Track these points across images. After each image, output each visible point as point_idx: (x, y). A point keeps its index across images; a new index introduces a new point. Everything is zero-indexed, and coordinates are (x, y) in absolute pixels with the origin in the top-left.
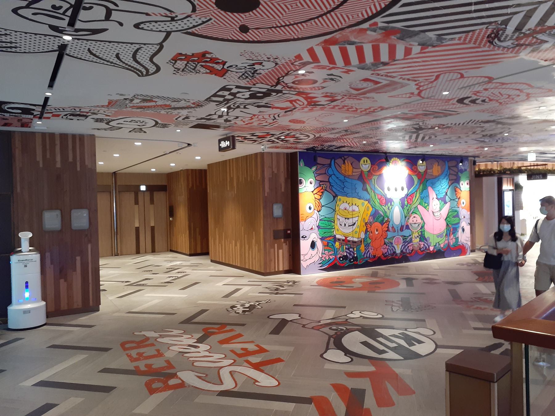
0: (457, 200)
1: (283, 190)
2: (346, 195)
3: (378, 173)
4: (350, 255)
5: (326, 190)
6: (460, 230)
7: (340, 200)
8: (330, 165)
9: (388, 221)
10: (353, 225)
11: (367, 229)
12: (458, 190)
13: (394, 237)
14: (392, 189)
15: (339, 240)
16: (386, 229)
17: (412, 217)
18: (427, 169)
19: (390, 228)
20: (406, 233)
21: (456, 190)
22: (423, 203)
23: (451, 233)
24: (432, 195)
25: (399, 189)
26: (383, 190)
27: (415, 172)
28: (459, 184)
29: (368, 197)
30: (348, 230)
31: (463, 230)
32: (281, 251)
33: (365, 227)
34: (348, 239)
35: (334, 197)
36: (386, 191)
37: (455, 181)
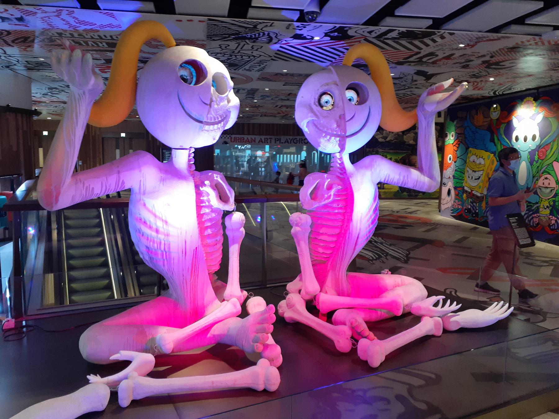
2: (476, 147)
3: (506, 121)
4: (473, 209)
5: (461, 142)
10: (478, 179)
14: (521, 139)
15: (466, 191)
26: (510, 139)
30: (474, 184)
34: (473, 192)
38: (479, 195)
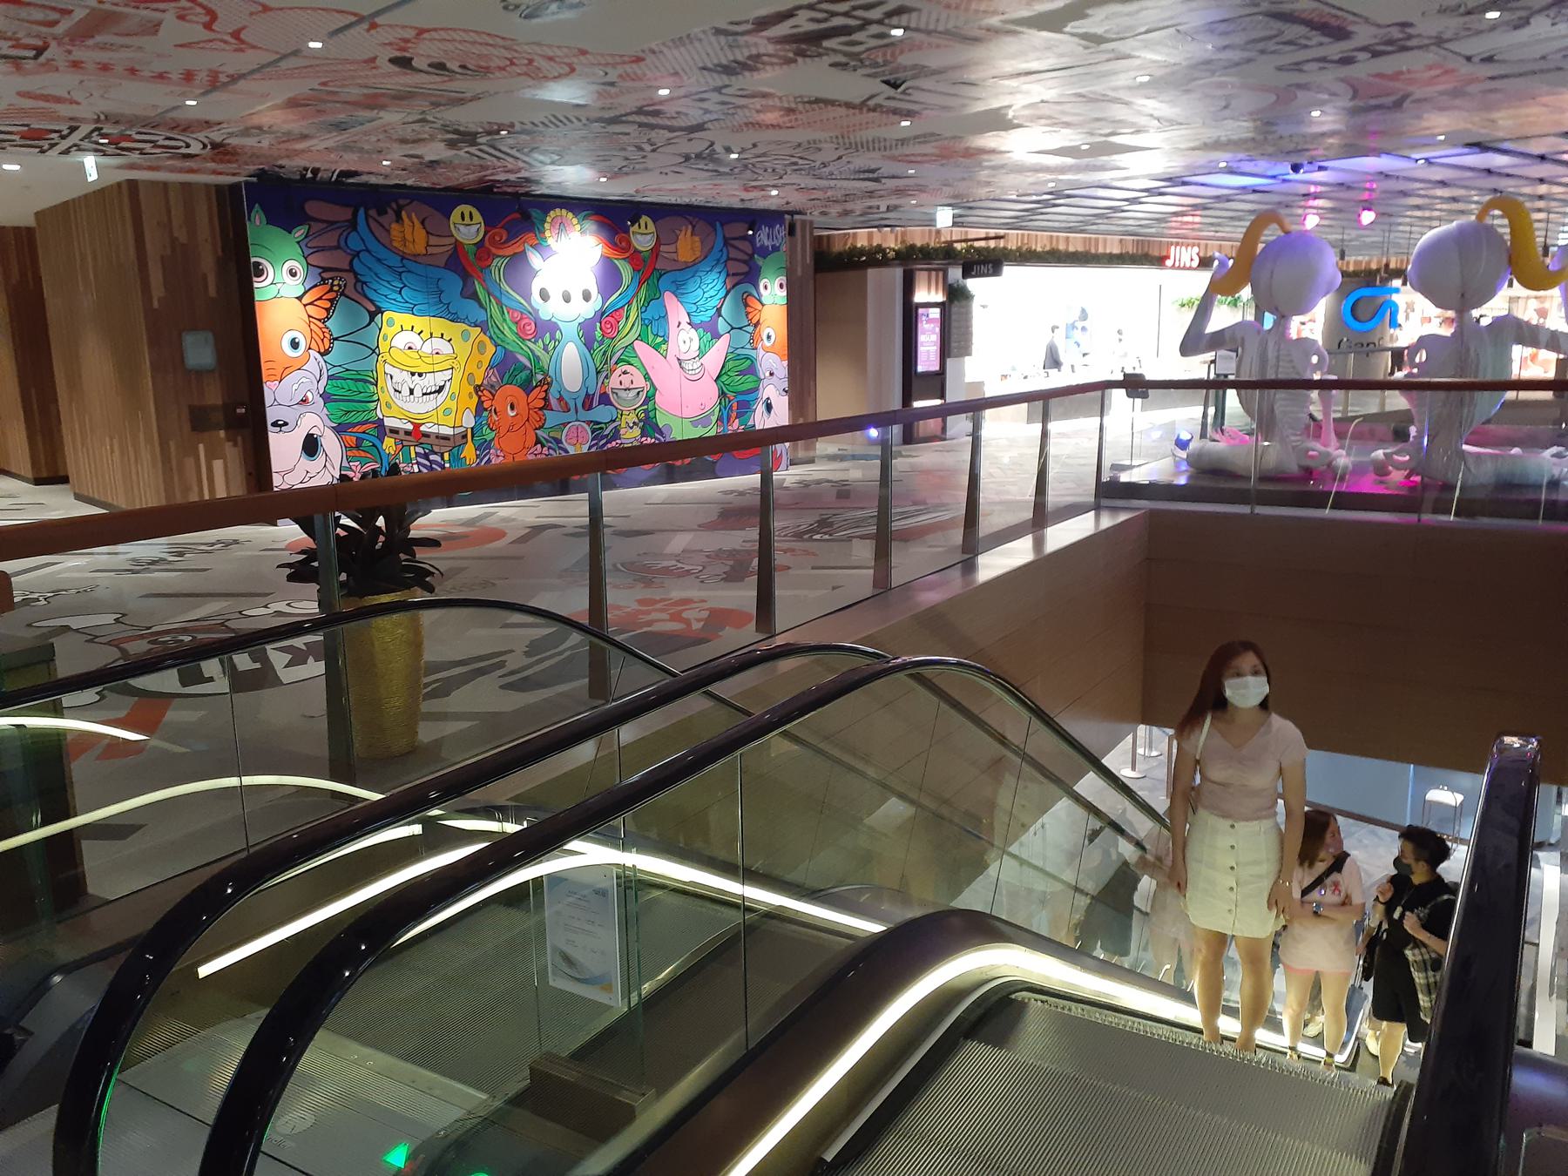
0: (750, 329)
1: (212, 292)
5: (343, 294)
6: (760, 408)
7: (391, 323)
8: (353, 225)
9: (546, 383)
11: (480, 403)
12: (751, 301)
13: (565, 425)
15: (394, 431)
16: (542, 403)
17: (618, 372)
18: (658, 243)
19: (553, 402)
20: (601, 413)
21: (747, 303)
22: (651, 337)
23: (734, 415)
24: (677, 312)
25: (577, 297)
26: (527, 297)
27: (624, 250)
28: (756, 287)
29: (481, 316)
30: (419, 407)
31: (769, 407)
32: (218, 465)
33: (475, 399)
35: (372, 316)
36: (536, 297)
37: (744, 277)
38: (450, 432)
